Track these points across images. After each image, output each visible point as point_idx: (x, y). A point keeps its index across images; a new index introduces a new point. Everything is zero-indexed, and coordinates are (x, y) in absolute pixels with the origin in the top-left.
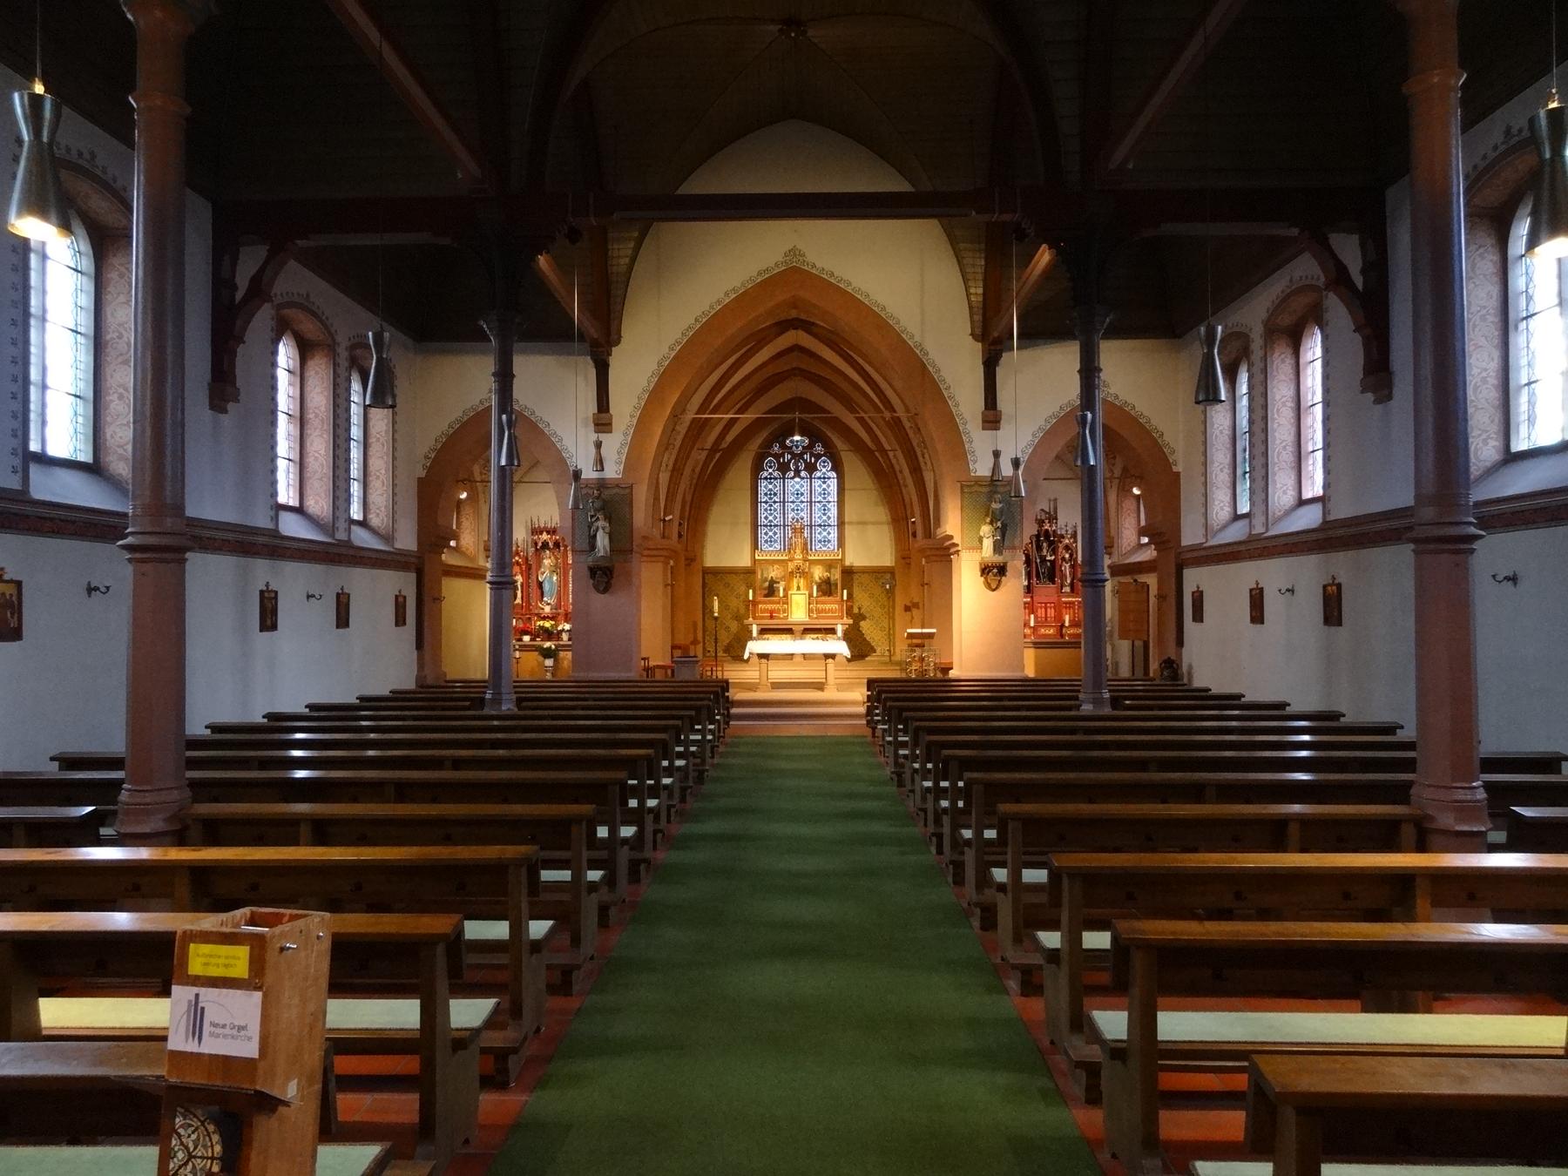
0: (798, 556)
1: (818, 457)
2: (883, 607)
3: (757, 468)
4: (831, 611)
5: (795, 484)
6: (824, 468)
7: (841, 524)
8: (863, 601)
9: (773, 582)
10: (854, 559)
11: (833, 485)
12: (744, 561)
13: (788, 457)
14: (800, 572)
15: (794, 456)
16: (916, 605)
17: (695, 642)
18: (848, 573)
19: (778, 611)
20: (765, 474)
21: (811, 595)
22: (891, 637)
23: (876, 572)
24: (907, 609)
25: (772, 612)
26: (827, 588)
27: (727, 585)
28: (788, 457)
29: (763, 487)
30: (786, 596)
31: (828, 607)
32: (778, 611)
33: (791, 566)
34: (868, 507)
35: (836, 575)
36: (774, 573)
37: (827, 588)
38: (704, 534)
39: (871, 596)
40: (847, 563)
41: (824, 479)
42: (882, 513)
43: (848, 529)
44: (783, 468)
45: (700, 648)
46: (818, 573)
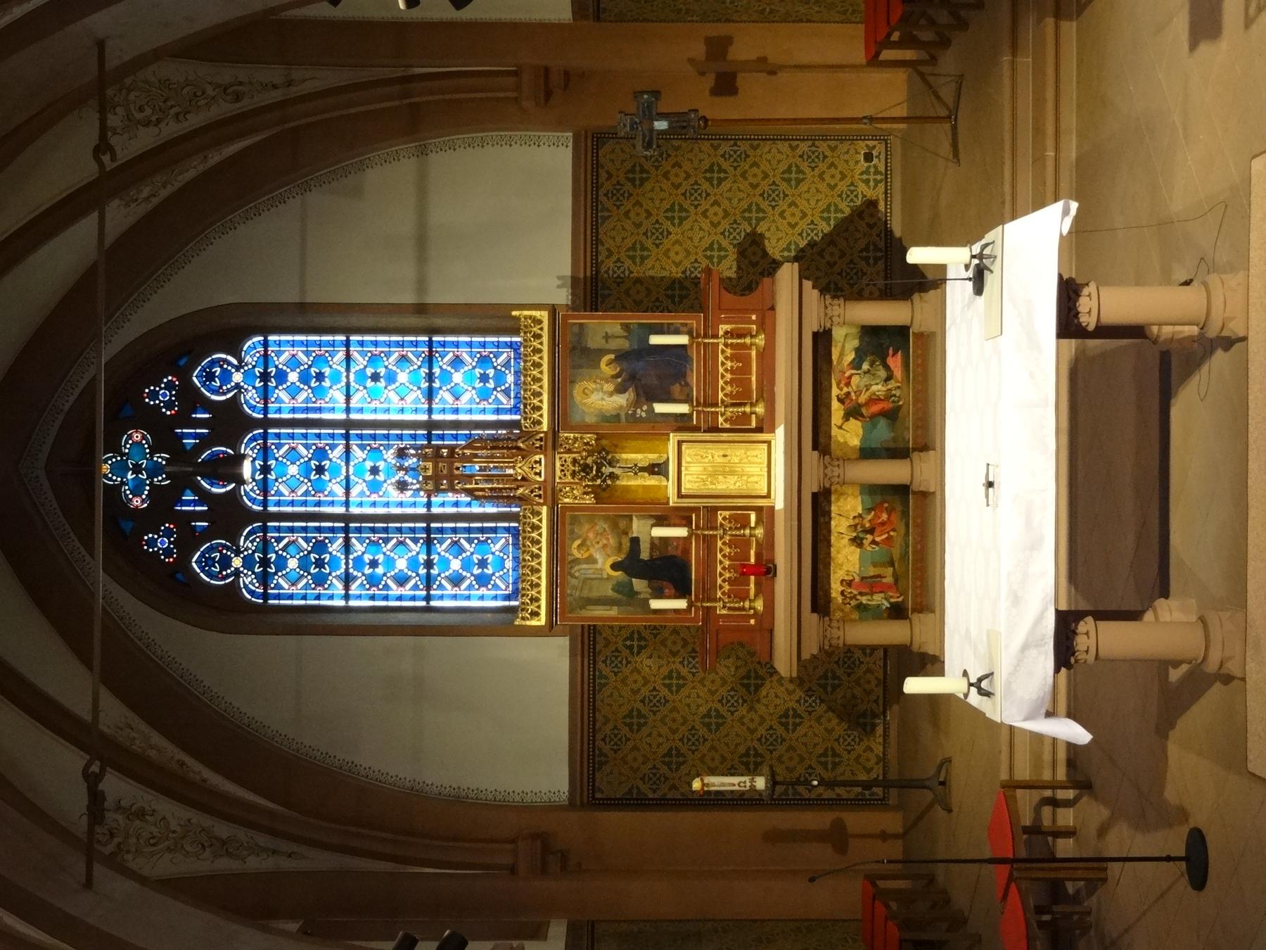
0: (536, 468)
1: (190, 398)
2: (715, 173)
3: (227, 609)
4: (740, 355)
5: (281, 478)
6: (235, 377)
7: (426, 320)
8: (694, 245)
9: (631, 564)
10: (540, 271)
11: (288, 349)
12: (555, 656)
13: (189, 504)
14: (596, 467)
15: (182, 482)
16: (719, 47)
17: (838, 838)
18: (593, 291)
19: (741, 544)
20: (248, 580)
21: (681, 424)
22: (826, 134)
23: (597, 198)
24: (726, 85)
25: (744, 571)
26: (652, 374)
27: (635, 720)
28: (189, 504)
29: (292, 589)
30: (682, 516)
31: (725, 365)
32: (741, 544)
33: (575, 496)
34: (362, 225)
35: (606, 329)
36: (599, 559)
37: (652, 374)
38: (458, 802)
39: (677, 214)
40: (562, 297)
41: (268, 378)
42: (388, 177)
43: (438, 295)
44: (230, 517)
45: (856, 821)
46: (599, 397)
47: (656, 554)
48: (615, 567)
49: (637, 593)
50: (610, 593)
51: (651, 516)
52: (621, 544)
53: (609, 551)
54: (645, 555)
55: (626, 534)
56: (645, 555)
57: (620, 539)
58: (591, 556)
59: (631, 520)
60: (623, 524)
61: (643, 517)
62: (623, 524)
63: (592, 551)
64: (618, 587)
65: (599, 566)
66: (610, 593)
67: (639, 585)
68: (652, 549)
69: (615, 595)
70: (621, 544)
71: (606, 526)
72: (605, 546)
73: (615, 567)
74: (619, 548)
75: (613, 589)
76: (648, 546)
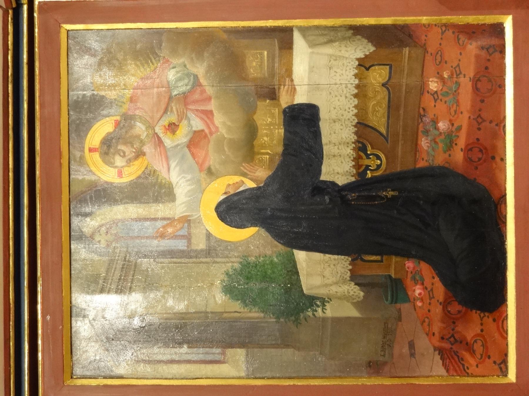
9: (294, 201)
47: (377, 165)
48: (231, 210)
49: (312, 301)
50: (218, 300)
51: (358, 31)
52: (251, 131)
53: (213, 159)
54: (337, 167)
55: (272, 95)
56: (337, 167)
57: (250, 111)
58: (150, 173)
59: (287, 45)
60: (257, 61)
61: (331, 35)
62: (257, 61)
63: (152, 158)
64: (247, 281)
65: (178, 208)
66: (218, 300)
67: (321, 272)
68: (361, 148)
69: (237, 306)
70: (251, 131)
71: (200, 69)
72: (196, 140)
73: (231, 210)
74: (248, 145)
75: (228, 290)
76: (348, 134)
